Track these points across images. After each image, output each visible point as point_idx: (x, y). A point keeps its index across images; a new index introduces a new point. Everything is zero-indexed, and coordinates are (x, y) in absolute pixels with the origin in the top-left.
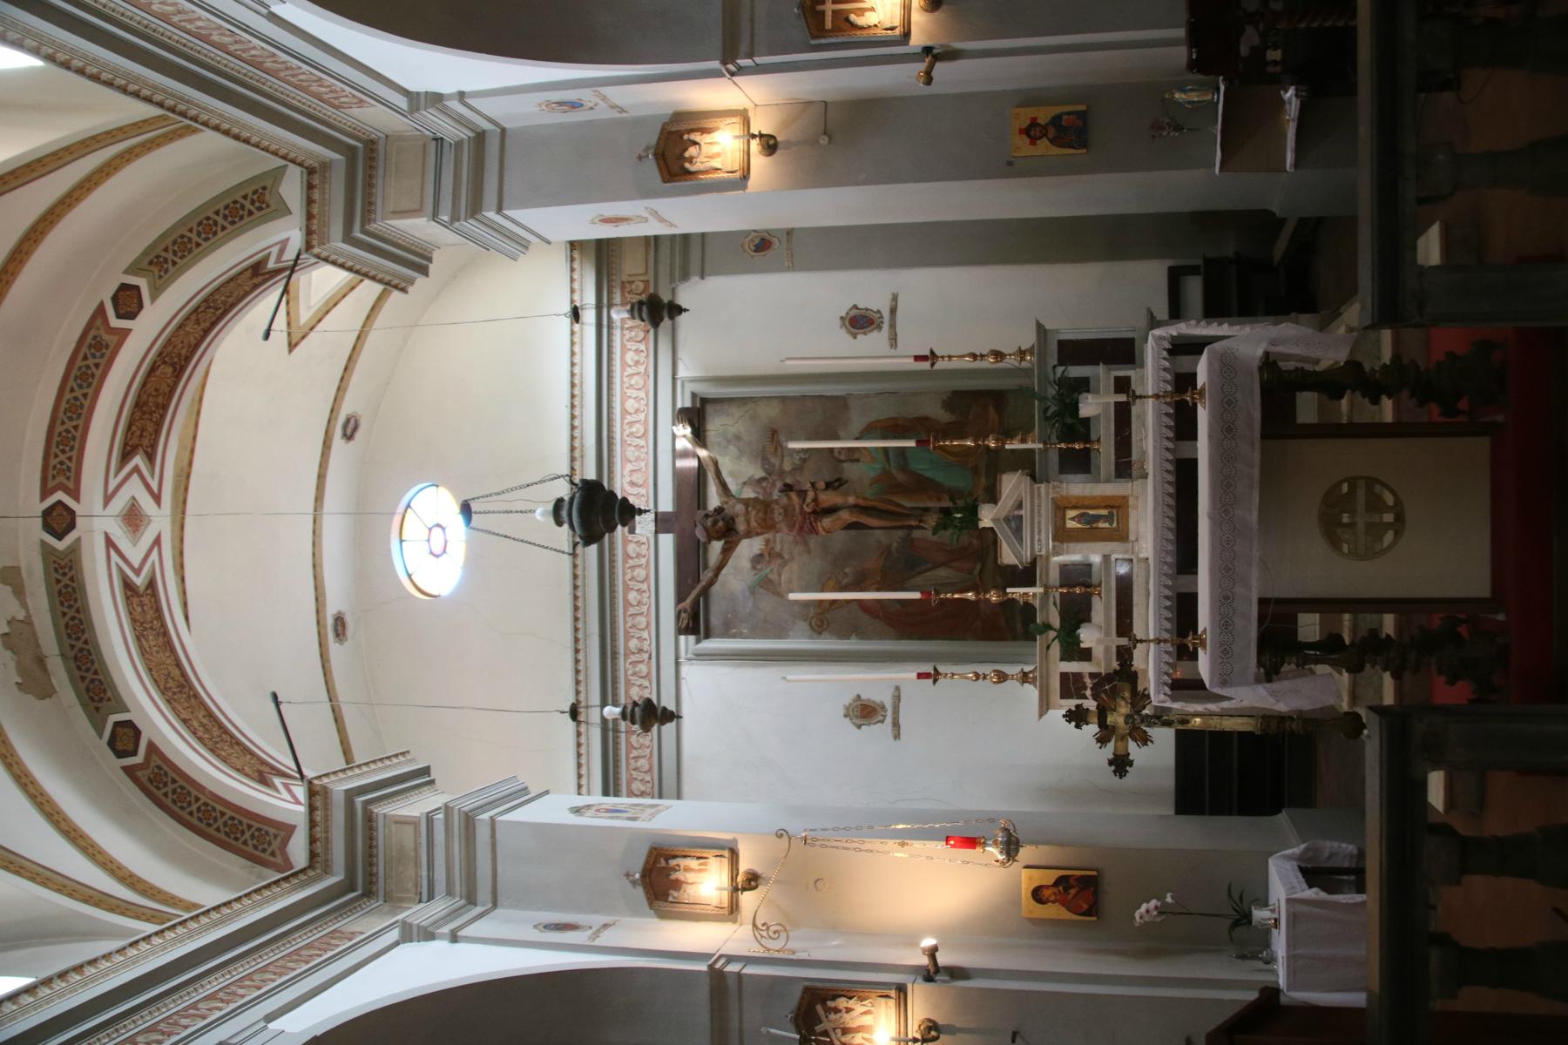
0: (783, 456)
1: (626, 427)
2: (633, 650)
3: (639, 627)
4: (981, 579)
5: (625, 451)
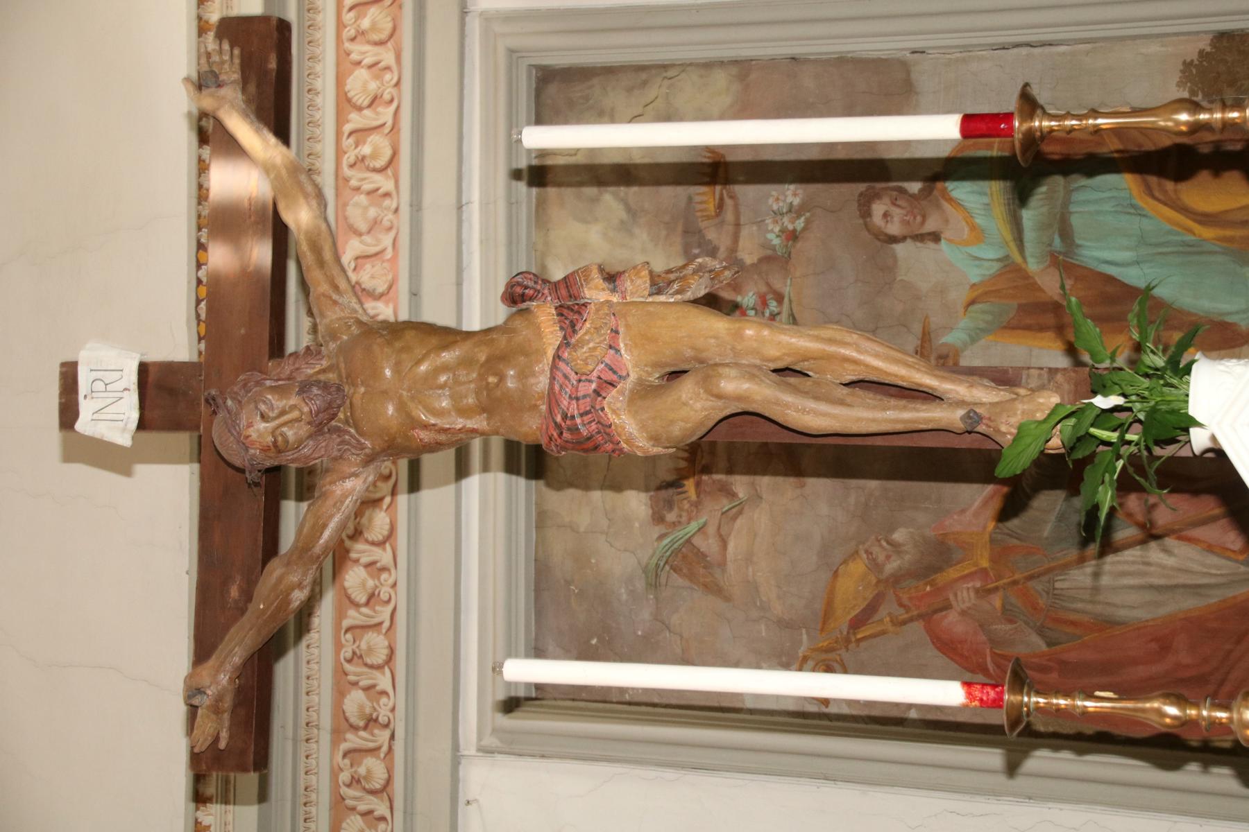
0: (737, 225)
1: (348, 143)
2: (353, 720)
3: (369, 661)
5: (345, 205)
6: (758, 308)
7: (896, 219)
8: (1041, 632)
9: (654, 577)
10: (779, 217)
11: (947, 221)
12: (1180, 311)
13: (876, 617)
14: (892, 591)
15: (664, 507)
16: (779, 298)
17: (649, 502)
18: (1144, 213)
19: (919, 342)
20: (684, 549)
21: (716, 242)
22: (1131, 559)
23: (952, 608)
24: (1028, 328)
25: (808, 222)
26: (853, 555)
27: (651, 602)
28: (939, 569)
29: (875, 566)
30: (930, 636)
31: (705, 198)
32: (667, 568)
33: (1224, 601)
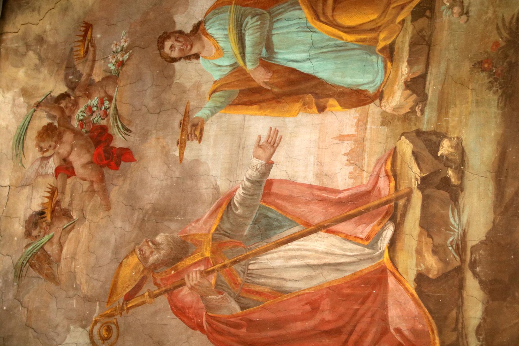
0: (94, 61)
4: (392, 259)
6: (99, 106)
7: (177, 49)
8: (238, 300)
9: (19, 271)
10: (117, 54)
11: (204, 47)
12: (334, 86)
13: (141, 293)
14: (151, 275)
15: (32, 227)
16: (110, 99)
17: (25, 224)
18: (314, 30)
19: (183, 118)
20: (39, 253)
21: (82, 71)
22: (297, 247)
23: (185, 285)
24: (244, 104)
25: (130, 56)
26: (132, 252)
27: (15, 287)
28: (180, 259)
29: (144, 259)
30: (171, 305)
31: (79, 48)
32: (28, 264)
33: (355, 274)
